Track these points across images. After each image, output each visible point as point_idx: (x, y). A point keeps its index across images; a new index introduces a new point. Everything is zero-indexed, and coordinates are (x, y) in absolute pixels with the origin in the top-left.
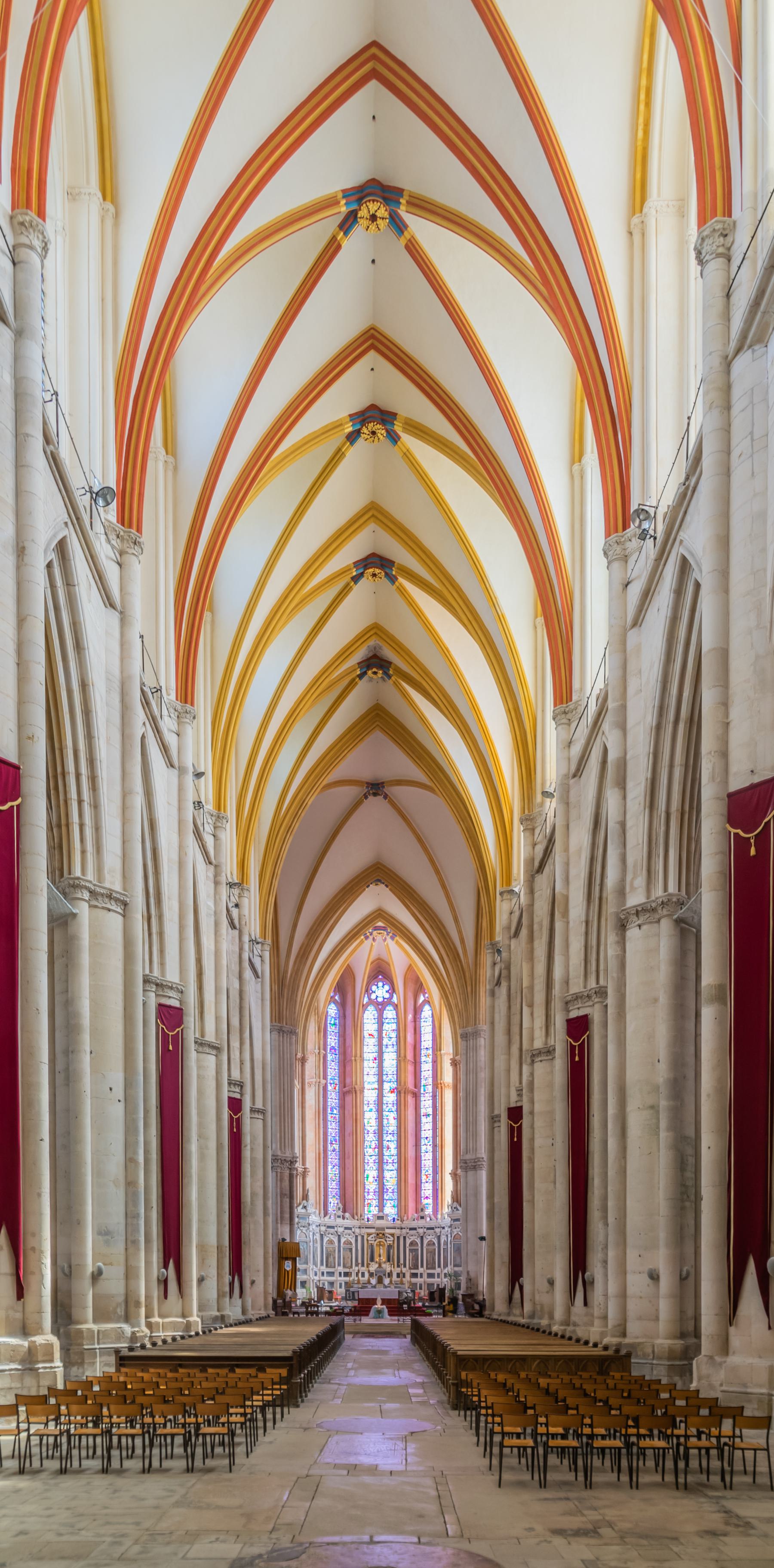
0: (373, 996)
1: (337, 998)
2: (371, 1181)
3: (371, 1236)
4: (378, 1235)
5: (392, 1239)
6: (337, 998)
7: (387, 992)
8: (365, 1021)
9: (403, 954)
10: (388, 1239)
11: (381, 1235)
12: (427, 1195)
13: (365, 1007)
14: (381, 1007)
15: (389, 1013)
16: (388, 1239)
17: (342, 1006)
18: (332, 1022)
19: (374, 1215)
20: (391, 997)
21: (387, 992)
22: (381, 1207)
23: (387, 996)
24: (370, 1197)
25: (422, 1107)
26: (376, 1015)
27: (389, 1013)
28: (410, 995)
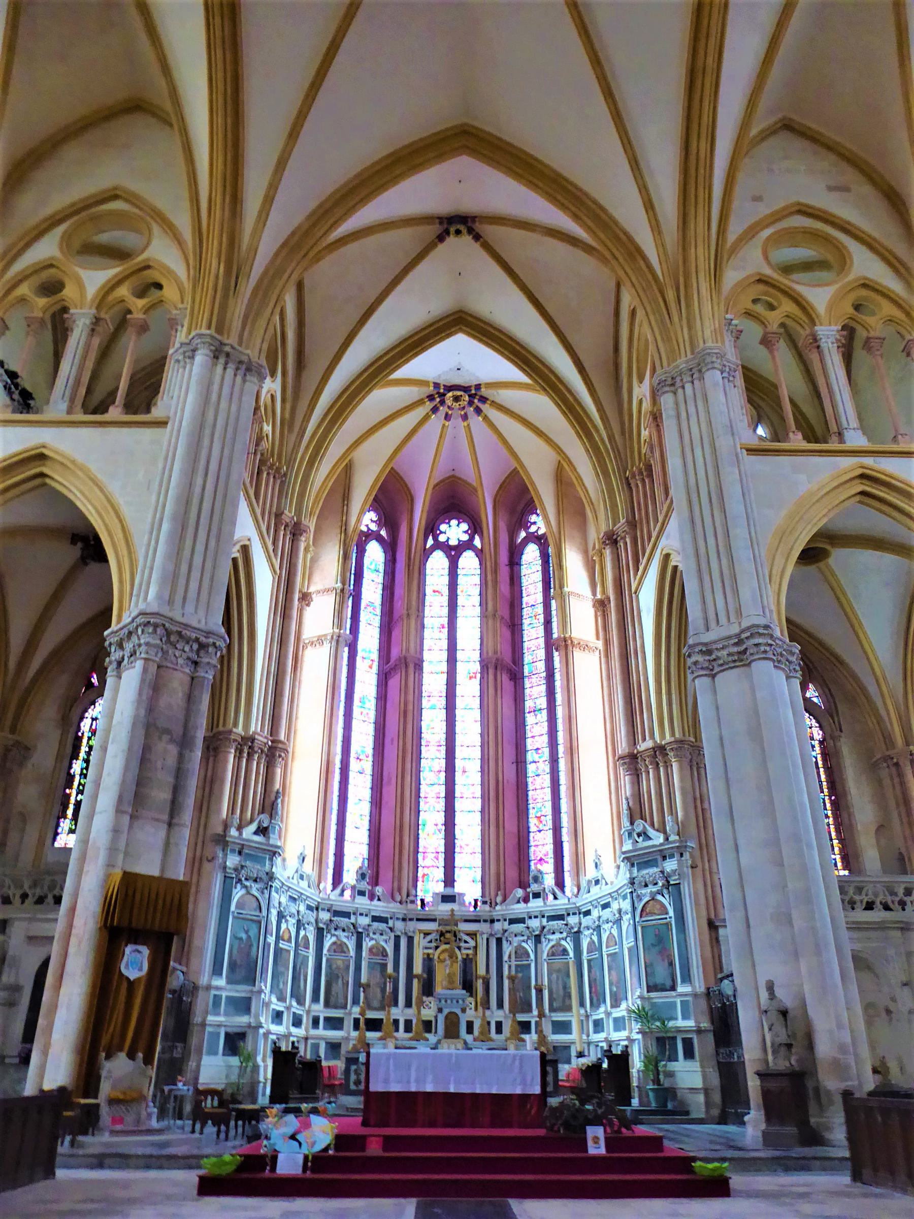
0: (442, 538)
1: (383, 533)
2: (431, 833)
4: (442, 934)
5: (472, 943)
6: (383, 533)
7: (466, 532)
9: (495, 437)
10: (462, 944)
12: (540, 856)
13: (426, 554)
14: (454, 553)
15: (469, 562)
16: (462, 944)
17: (390, 548)
18: (373, 567)
20: (472, 539)
21: (466, 532)
22: (449, 880)
23: (465, 537)
24: (428, 862)
25: (527, 698)
27: (469, 562)
28: (502, 526)
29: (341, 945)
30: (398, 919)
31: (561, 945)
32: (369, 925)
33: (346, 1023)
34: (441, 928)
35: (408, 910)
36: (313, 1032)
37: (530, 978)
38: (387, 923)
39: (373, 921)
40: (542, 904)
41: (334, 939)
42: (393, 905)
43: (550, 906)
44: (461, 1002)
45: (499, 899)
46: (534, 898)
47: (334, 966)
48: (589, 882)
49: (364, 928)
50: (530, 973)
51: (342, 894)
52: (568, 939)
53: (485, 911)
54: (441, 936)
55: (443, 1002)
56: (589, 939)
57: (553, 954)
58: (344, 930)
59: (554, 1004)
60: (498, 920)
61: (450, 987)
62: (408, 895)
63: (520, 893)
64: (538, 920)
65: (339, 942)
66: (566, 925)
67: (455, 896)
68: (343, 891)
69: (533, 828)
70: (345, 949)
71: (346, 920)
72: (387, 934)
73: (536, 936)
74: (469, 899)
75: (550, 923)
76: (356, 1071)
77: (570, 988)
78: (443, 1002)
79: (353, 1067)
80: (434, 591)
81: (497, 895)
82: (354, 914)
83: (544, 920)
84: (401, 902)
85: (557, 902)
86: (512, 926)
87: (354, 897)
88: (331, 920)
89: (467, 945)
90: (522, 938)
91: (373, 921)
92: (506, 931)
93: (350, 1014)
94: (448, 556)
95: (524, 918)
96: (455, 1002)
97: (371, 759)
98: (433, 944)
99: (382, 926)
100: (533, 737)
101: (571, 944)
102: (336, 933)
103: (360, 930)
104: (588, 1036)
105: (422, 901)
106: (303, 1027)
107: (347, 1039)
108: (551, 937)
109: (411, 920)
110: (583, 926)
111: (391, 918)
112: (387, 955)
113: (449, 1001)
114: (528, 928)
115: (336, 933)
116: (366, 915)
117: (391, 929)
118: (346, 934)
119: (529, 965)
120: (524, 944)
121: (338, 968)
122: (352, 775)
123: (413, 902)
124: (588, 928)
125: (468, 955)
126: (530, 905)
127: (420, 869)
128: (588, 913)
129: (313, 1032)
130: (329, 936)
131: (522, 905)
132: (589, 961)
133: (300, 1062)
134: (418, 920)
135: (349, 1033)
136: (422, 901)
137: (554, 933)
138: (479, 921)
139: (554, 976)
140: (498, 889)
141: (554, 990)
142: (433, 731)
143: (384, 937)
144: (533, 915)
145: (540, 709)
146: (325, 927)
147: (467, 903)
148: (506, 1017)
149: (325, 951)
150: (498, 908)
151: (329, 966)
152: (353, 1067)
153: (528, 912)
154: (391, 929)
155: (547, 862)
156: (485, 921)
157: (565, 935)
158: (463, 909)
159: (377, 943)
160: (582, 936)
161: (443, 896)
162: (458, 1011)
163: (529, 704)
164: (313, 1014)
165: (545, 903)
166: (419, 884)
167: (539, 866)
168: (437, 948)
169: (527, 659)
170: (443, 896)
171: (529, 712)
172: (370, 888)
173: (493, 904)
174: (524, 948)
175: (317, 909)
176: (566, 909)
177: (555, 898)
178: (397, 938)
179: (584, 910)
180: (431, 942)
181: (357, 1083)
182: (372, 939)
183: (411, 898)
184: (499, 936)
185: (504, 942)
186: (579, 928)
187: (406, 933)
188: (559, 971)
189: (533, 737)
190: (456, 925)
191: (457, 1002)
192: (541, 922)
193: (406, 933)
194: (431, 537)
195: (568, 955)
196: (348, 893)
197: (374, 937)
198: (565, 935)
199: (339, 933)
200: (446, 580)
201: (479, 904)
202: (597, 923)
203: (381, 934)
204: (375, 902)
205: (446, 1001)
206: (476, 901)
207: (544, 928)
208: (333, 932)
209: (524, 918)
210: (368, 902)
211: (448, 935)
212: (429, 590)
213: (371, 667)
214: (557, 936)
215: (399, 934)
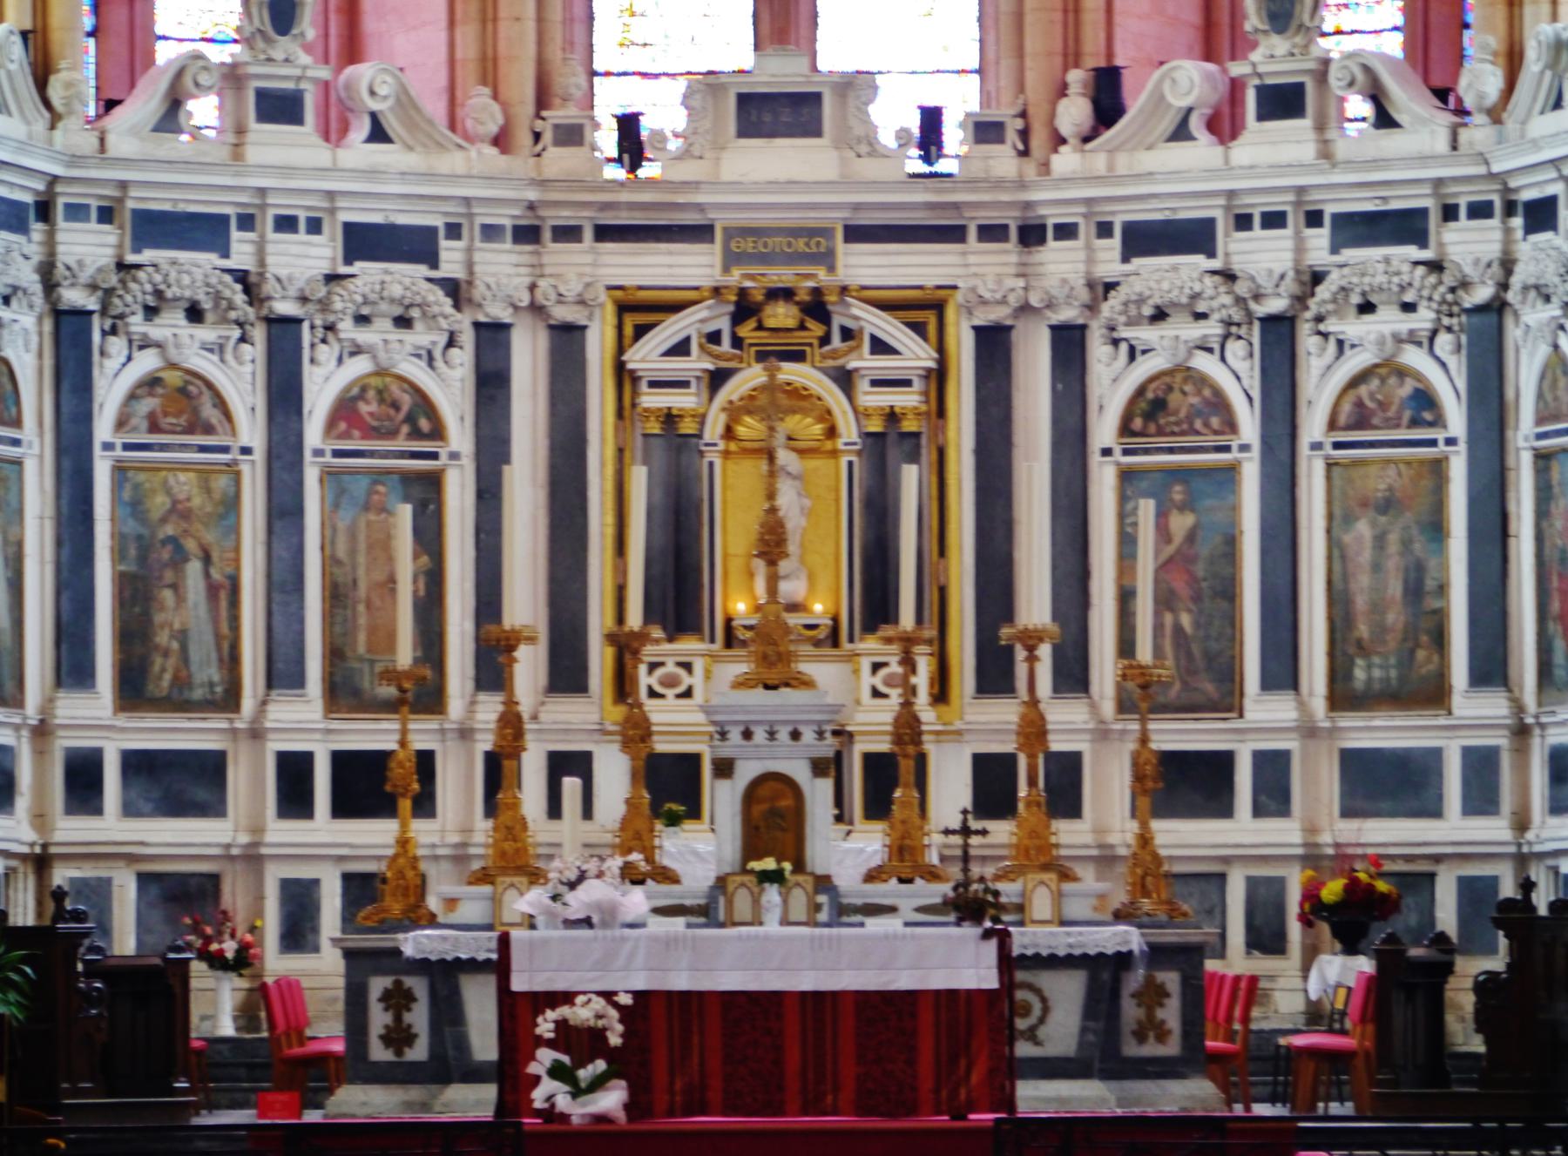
3: (671, 329)
4: (745, 309)
5: (916, 354)
10: (864, 362)
11: (781, 315)
16: (864, 362)
19: (707, 85)
29: (183, 391)
30: (491, 232)
31: (1402, 373)
32: (332, 278)
33: (237, 778)
34: (736, 277)
35: (542, 183)
36: (72, 830)
37: (1231, 544)
38: (433, 261)
39: (349, 260)
40: (1307, 151)
41: (147, 362)
42: (453, 162)
43: (1350, 164)
44: (808, 735)
45: (1075, 112)
46: (1261, 117)
47: (160, 502)
49: (304, 300)
50: (1235, 509)
51: (171, 115)
52: (1444, 341)
53: (999, 184)
54: (738, 317)
55: (735, 735)
56: (1544, 350)
57: (1362, 420)
58: (195, 314)
59: (1360, 674)
60: (1066, 231)
61: (773, 676)
62: (543, 99)
64: (1281, 239)
65: (173, 378)
66: (1436, 266)
67: (817, 97)
68: (174, 103)
70: (209, 412)
71: (209, 259)
72: (431, 319)
73: (1269, 321)
75: (1351, 254)
76: (386, 997)
77: (1442, 589)
78: (735, 735)
79: (378, 985)
81: (1062, 91)
82: (247, 222)
83: (1319, 239)
84: (501, 141)
85: (1390, 142)
86: (1137, 262)
87: (240, 131)
88: (121, 266)
89: (883, 362)
90: (1195, 331)
91: (349, 260)
92: (1110, 287)
93: (256, 734)
95: (1209, 224)
96: (783, 734)
98: (697, 363)
99: (405, 277)
101: (1459, 366)
102: (156, 331)
103: (285, 308)
104: (1521, 824)
105: (628, 125)
106: (22, 803)
107: (253, 858)
108: (1352, 327)
109: (567, 233)
110: (1516, 281)
111: (454, 231)
112: (438, 433)
113: (760, 735)
114: (1229, 276)
115: (156, 331)
116: (315, 226)
117: (455, 290)
118: (206, 333)
119: (1231, 472)
120: (1205, 364)
121: (179, 511)
123: (572, 135)
125: (892, 416)
128: (1541, 215)
129: (72, 830)
130: (117, 345)
131: (1202, 150)
132: (1543, 459)
133: (93, 971)
134: (605, 233)
135: (258, 829)
136: (628, 125)
137: (1367, 308)
138: (954, 234)
139: (1363, 529)
140: (1072, 57)
141: (1361, 602)
143: (421, 336)
144: (1258, 206)
146: (92, 304)
147: (887, 139)
148: (1102, 734)
149: (103, 429)
150: (1066, 161)
151: (131, 504)
152: (378, 985)
153: (1231, 194)
154: (455, 290)
156: (993, 233)
157: (1423, 319)
158: (869, 169)
159: (381, 372)
160: (1513, 333)
161: (745, 100)
162: (799, 771)
164: (65, 741)
165: (1326, 152)
168: (717, 379)
170: (745, 100)
172: (324, 73)
173: (1038, 140)
174: (1202, 380)
175: (44, 210)
176: (1438, 183)
177: (1384, 120)
178: (492, 336)
179: (1528, 195)
180: (680, 349)
181: (399, 1037)
182: (357, 351)
183: (559, 114)
184: (1068, 314)
185: (1098, 350)
186: (1504, 286)
187: (536, 309)
188: (1388, 505)
190: (827, 259)
191: (795, 735)
192: (1300, 249)
193: (536, 309)
195: (1439, 422)
196: (203, 110)
197: (364, 336)
198: (1423, 319)
199: (171, 326)
201: (953, 137)
203: (403, 322)
205: (747, 735)
206: (932, 119)
207: (1317, 278)
208: (137, 323)
209: (1209, 224)
210: (320, 154)
211: (781, 315)
214: (1388, 321)
215: (505, 316)
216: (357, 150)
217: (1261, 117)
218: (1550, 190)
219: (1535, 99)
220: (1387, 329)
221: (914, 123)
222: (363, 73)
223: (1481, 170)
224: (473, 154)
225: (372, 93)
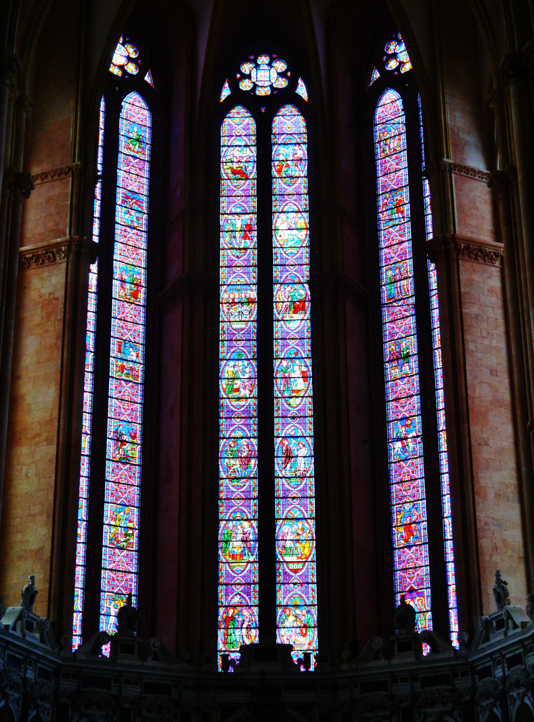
1: (147, 78)
6: (147, 78)
8: (224, 141)
12: (410, 583)
20: (293, 85)
21: (282, 75)
23: (282, 83)
26: (253, 128)
40: (413, 659)
46: (399, 651)
48: (488, 623)
52: (456, 713)
56: (488, 713)
63: (378, 642)
69: (399, 542)
74: (296, 655)
80: (234, 172)
83: (418, 685)
94: (255, 115)
97: (138, 440)
100: (396, 400)
103: (126, 706)
108: (429, 711)
122: (110, 466)
124: (486, 695)
126: (394, 662)
127: (221, 610)
131: (382, 662)
136: (225, 658)
142: (236, 394)
145: (408, 356)
150: (344, 667)
155: (421, 595)
157: (450, 706)
163: (389, 348)
166: (221, 633)
167: (408, 601)
169: (387, 274)
171: (390, 361)
189: (396, 400)
194: (227, 85)
198: (450, 706)
200: (251, 153)
201: (313, 660)
202: (501, 688)
204: (150, 663)
206: (307, 656)
210: (139, 663)
212: (225, 170)
213: (135, 295)
214: (438, 709)
216: (150, 663)
217: (399, 651)
218: (488, 664)
219: (480, 640)
220: (439, 710)
221: (302, 656)
222: (153, 640)
223: (465, 661)
224: (182, 664)
225: (154, 646)
